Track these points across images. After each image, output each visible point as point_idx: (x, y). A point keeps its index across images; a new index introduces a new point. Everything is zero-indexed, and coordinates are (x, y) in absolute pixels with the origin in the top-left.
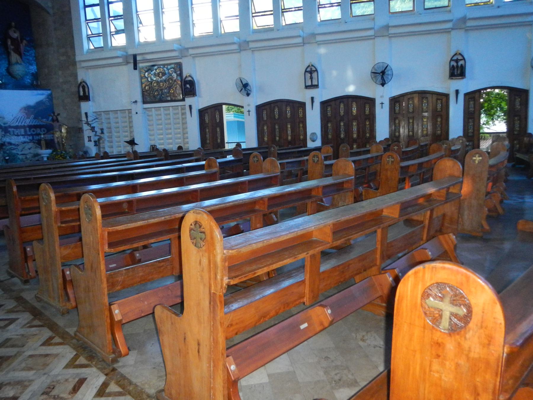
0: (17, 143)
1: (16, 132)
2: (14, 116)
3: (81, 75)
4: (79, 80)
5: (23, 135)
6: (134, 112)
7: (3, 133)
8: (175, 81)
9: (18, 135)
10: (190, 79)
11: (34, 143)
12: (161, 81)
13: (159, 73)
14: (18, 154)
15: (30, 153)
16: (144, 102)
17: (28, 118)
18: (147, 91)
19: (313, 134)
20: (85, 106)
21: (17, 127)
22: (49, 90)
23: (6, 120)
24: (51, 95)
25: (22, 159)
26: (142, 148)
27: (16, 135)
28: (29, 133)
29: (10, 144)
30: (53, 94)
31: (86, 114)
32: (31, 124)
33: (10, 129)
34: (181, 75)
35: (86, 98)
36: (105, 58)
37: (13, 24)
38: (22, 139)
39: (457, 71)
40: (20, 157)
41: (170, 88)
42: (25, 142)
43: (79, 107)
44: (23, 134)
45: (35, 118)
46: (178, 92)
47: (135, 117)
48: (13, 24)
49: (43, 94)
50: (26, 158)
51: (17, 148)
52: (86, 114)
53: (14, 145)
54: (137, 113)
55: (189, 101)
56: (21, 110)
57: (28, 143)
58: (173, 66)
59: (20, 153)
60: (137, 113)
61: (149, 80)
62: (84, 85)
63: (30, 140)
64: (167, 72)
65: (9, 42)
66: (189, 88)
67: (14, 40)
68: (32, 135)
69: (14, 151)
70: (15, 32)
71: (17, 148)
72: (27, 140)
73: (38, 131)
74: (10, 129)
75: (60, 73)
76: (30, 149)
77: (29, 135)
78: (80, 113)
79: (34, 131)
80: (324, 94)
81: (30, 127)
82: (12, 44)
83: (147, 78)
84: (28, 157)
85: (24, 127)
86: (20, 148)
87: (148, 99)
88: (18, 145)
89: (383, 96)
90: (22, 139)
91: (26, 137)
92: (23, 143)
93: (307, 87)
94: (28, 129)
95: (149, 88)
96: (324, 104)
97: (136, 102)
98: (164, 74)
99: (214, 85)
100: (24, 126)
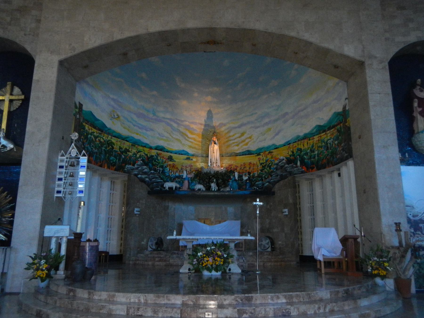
7: (412, 230)
65: (416, 104)
82: (419, 106)
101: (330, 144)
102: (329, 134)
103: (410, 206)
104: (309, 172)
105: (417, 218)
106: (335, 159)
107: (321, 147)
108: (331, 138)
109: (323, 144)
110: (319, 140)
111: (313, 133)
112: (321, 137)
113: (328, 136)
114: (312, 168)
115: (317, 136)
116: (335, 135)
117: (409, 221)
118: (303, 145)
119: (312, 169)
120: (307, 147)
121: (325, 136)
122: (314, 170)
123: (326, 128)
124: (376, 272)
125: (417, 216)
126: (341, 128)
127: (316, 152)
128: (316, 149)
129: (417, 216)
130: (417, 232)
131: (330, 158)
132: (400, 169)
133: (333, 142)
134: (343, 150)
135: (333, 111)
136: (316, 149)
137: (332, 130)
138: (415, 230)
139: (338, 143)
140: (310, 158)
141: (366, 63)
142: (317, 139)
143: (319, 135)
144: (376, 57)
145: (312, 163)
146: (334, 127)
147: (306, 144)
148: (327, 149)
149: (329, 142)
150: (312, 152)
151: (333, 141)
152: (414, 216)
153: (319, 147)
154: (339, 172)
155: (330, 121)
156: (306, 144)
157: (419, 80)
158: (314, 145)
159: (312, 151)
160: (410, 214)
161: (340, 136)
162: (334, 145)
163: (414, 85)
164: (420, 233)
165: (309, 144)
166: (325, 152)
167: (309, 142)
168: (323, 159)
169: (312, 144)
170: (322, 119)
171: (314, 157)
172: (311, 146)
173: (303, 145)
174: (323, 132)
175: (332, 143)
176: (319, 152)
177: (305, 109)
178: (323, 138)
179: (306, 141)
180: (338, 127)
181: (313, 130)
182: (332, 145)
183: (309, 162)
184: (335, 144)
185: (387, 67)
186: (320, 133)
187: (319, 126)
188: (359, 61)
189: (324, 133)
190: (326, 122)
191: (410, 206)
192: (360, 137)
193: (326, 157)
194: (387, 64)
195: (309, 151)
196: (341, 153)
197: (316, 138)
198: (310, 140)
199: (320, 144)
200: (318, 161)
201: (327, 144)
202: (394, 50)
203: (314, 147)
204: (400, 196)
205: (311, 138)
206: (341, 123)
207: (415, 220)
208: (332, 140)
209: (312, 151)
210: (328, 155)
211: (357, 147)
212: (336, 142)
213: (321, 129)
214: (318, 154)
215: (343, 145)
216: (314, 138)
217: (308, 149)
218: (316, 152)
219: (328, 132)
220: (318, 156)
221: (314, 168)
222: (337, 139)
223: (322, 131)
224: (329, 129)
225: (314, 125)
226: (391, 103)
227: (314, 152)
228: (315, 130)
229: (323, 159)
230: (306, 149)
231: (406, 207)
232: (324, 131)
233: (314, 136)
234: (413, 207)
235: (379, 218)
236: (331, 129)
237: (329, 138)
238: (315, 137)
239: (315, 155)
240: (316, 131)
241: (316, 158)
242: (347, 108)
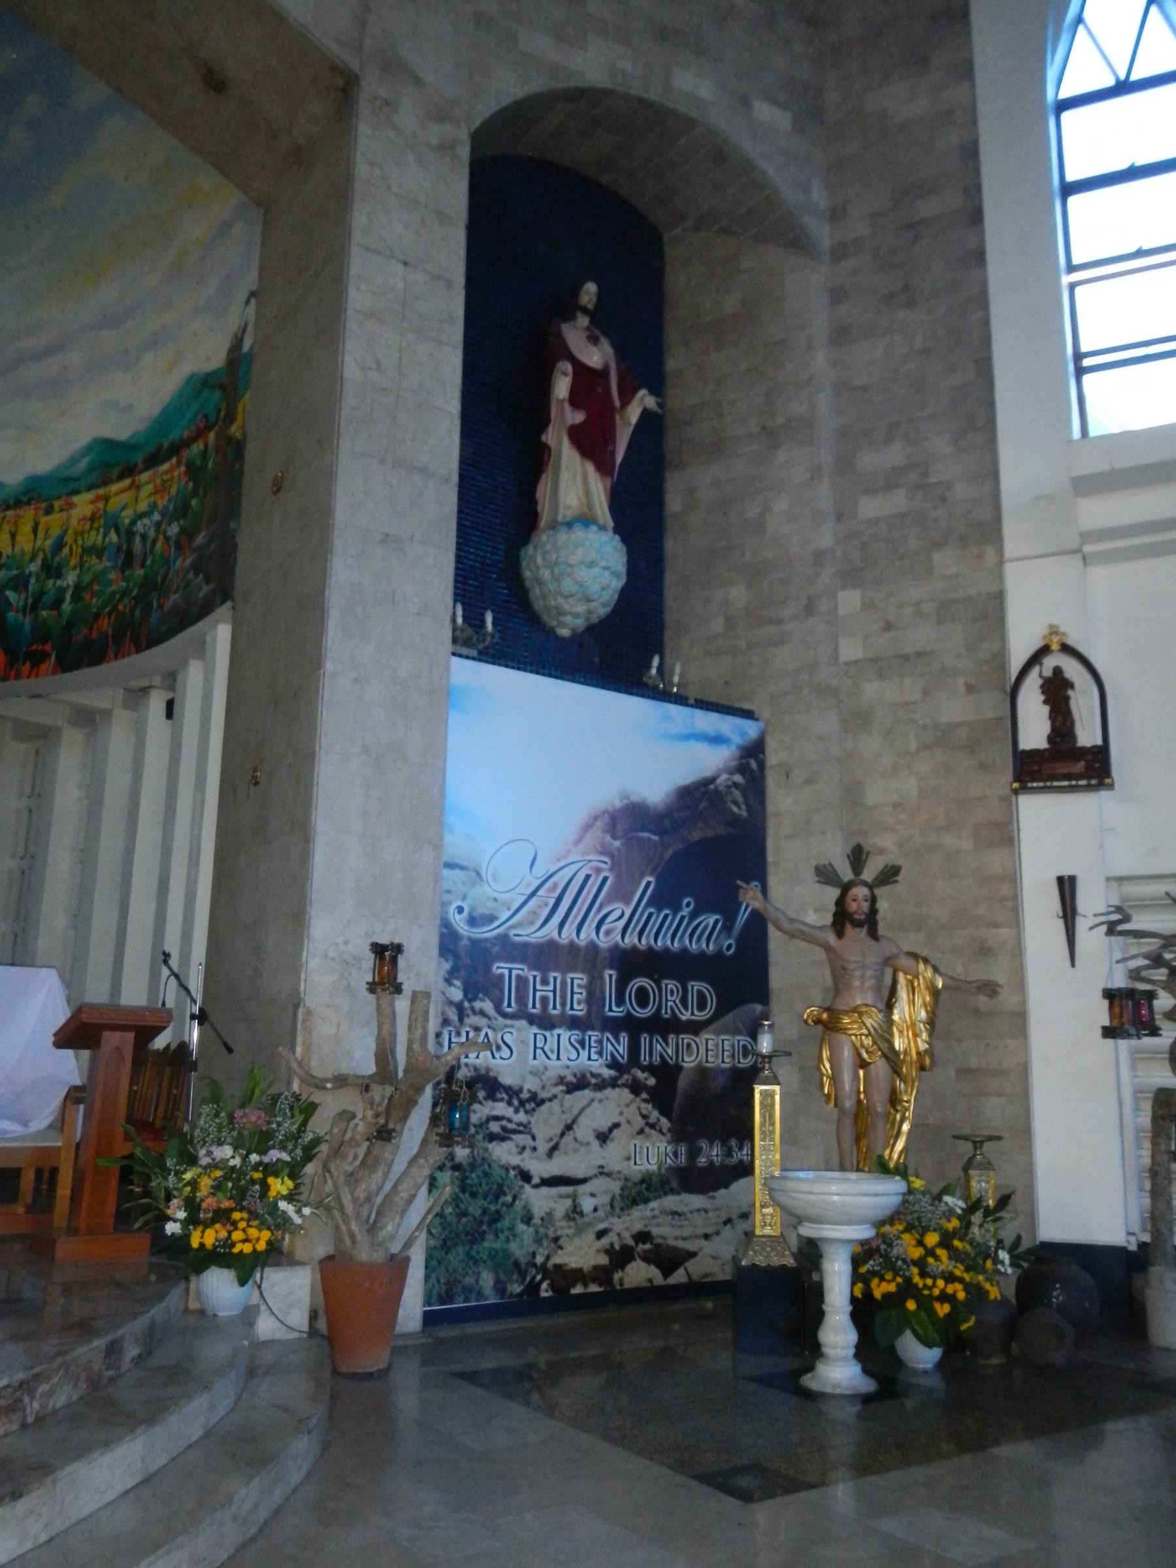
0: (531, 1084)
1: (544, 990)
2: (541, 870)
3: (1036, 604)
5: (574, 1023)
7: (457, 994)
9: (545, 1022)
11: (636, 1088)
14: (526, 1176)
15: (603, 1172)
17: (621, 893)
20: (1053, 830)
21: (545, 956)
22: (748, 715)
23: (482, 896)
24: (754, 751)
25: (548, 1218)
27: (532, 1020)
28: (617, 1012)
29: (488, 1085)
30: (771, 745)
31: (1067, 887)
32: (631, 940)
33: (500, 968)
37: (589, 292)
38: (567, 1054)
40: (540, 1200)
42: (579, 1083)
43: (1004, 835)
44: (580, 1010)
45: (658, 901)
48: (589, 292)
49: (717, 740)
50: (575, 1212)
51: (524, 1128)
52: (1067, 887)
53: (512, 1093)
56: (587, 828)
57: (603, 1085)
59: (539, 1168)
63: (614, 1064)
65: (562, 387)
67: (585, 379)
68: (632, 1026)
69: (503, 1153)
70: (594, 340)
71: (524, 1128)
72: (598, 1066)
73: (669, 997)
74: (500, 968)
75: (849, 600)
76: (603, 1138)
77: (613, 1026)
78: (1013, 878)
79: (642, 998)
81: (630, 963)
82: (575, 400)
84: (587, 1204)
85: (586, 958)
86: (546, 1123)
88: (536, 1101)
90: (567, 1054)
91: (594, 1035)
92: (572, 1088)
94: (610, 975)
100: (593, 947)
101: (144, 537)
102: (149, 488)
103: (462, 868)
104: (18, 677)
105: (485, 932)
106: (155, 617)
107: (99, 552)
108: (153, 506)
109: (113, 537)
110: (92, 519)
111: (67, 480)
112: (106, 499)
113: (139, 500)
114: (37, 659)
115: (90, 495)
116: (174, 490)
117: (448, 942)
118: (13, 536)
119: (32, 667)
120: (28, 548)
121: (127, 496)
122: (44, 667)
123: (139, 458)
124: (209, 1237)
125: (491, 919)
126: (204, 454)
127: (71, 578)
128: (73, 562)
129: (491, 919)
130: (478, 1005)
131: (132, 611)
132: (447, 668)
133: (157, 531)
134: (197, 568)
135: (186, 369)
136: (73, 562)
137: (165, 467)
138: (471, 992)
139: (183, 531)
140: (35, 608)
141: (363, 84)
142: (88, 510)
143: (101, 491)
144: (418, 81)
145: (42, 633)
146: (176, 449)
147: (26, 529)
148: (128, 561)
149: (139, 527)
150: (49, 576)
151: (158, 524)
152: (472, 921)
153: (86, 551)
154: (170, 696)
155: (164, 420)
156: (26, 529)
157: (591, 288)
158: (69, 538)
159: (51, 570)
160: (460, 910)
161: (195, 493)
162: (159, 546)
163: (568, 309)
164: (488, 1006)
165: (41, 534)
166: (116, 582)
167: (43, 520)
168: (97, 616)
169: (55, 532)
170: (129, 408)
171: (57, 603)
172: (49, 542)
173: (13, 536)
174: (121, 477)
175: (152, 534)
176: (87, 579)
177: (50, 350)
178: (115, 503)
179: (29, 513)
180: (197, 447)
181: (74, 460)
182: (154, 542)
183: (27, 627)
184: (167, 539)
185: (464, 152)
186: (105, 482)
187: (109, 445)
188: (336, 69)
189: (127, 482)
190: (142, 426)
191: (462, 868)
192: (278, 488)
193: (115, 608)
194: (464, 134)
195: (34, 567)
196: (188, 585)
197: (83, 504)
198: (49, 511)
199: (94, 538)
200: (69, 626)
201: (130, 534)
202: (508, 87)
203: (66, 550)
204: (427, 815)
205: (57, 504)
206: (209, 428)
207: (474, 942)
208: (156, 517)
209: (51, 570)
210: (125, 593)
211: (259, 540)
212: (174, 529)
213: (114, 462)
214: (78, 589)
215: (200, 539)
216: (71, 505)
217: (33, 558)
218: (71, 578)
219: (145, 477)
220: (77, 597)
221: (44, 656)
222: (182, 510)
223: (115, 473)
224: (153, 460)
225: (84, 440)
226: (457, 332)
227: (58, 574)
228: (83, 464)
229: (97, 616)
230: (23, 553)
231: (446, 872)
232: (129, 471)
233: (77, 492)
234: (479, 874)
235: (298, 920)
236: (163, 461)
237: (143, 506)
238: (76, 499)
239: (62, 591)
240: (91, 469)
241: (67, 607)
242: (246, 347)
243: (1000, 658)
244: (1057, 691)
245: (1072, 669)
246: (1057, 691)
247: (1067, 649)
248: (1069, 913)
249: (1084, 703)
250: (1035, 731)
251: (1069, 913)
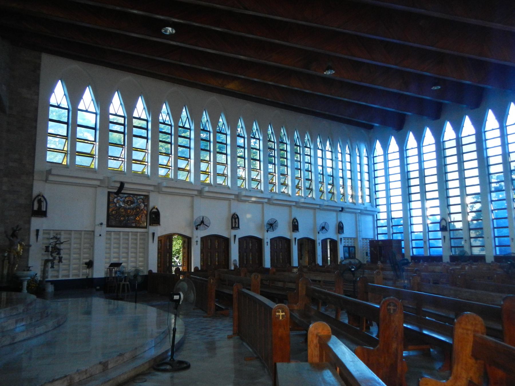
3: (38, 188)
4: (36, 192)
6: (97, 234)
8: (142, 210)
10: (155, 210)
12: (129, 209)
13: (128, 201)
16: (108, 225)
18: (113, 215)
19: (235, 260)
20: (36, 223)
26: (99, 272)
31: (38, 231)
34: (147, 206)
35: (42, 213)
36: (69, 175)
39: (295, 227)
41: (137, 215)
43: (29, 222)
46: (143, 220)
47: (97, 239)
54: (100, 235)
55: (152, 229)
58: (142, 197)
60: (100, 235)
61: (118, 205)
62: (41, 199)
64: (136, 201)
66: (155, 218)
75: (5, 179)
80: (241, 233)
83: (116, 204)
87: (114, 223)
89: (268, 237)
93: (233, 228)
95: (116, 213)
96: (240, 239)
97: (101, 224)
98: (133, 203)
99: (174, 219)
243: (31, 195)
244: (40, 202)
245: (42, 199)
246: (40, 202)
247: (43, 196)
248: (37, 235)
249: (44, 204)
250: (36, 208)
251: (37, 235)
